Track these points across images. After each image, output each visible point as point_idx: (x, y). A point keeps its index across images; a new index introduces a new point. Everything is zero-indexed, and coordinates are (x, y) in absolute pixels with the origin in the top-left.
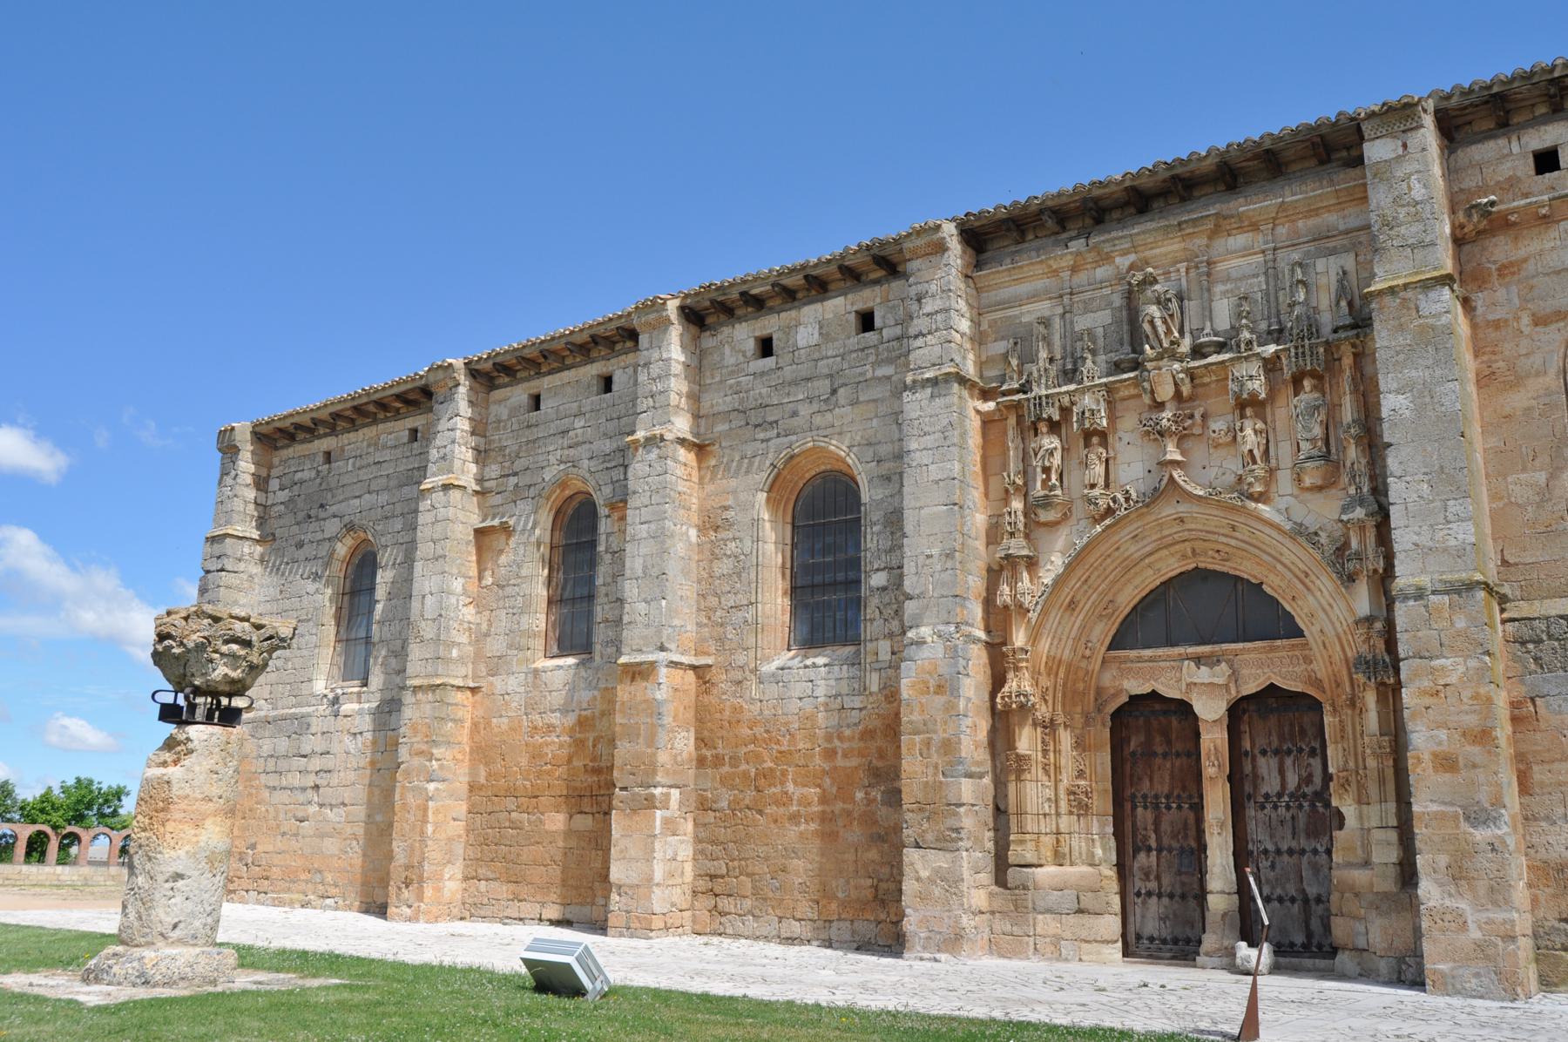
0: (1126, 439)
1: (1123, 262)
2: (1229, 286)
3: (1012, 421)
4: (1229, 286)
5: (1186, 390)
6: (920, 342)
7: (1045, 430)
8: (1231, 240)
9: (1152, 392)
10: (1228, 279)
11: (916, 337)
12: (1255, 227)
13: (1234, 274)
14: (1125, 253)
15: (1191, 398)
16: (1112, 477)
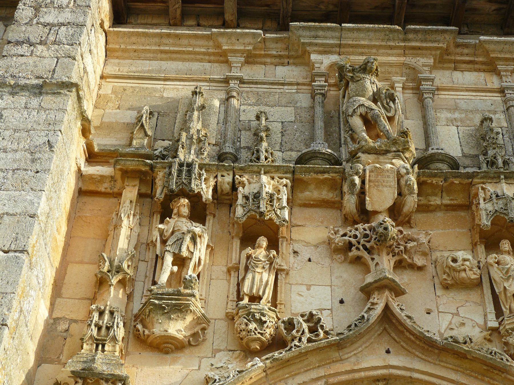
0: (306, 253)
1: (323, 61)
2: (457, 115)
3: (130, 193)
4: (457, 115)
5: (411, 201)
6: (24, 49)
7: (185, 211)
8: (457, 75)
9: (362, 193)
10: (456, 108)
11: (18, 43)
12: (491, 67)
13: (463, 105)
14: (326, 50)
15: (407, 222)
16: (280, 297)
